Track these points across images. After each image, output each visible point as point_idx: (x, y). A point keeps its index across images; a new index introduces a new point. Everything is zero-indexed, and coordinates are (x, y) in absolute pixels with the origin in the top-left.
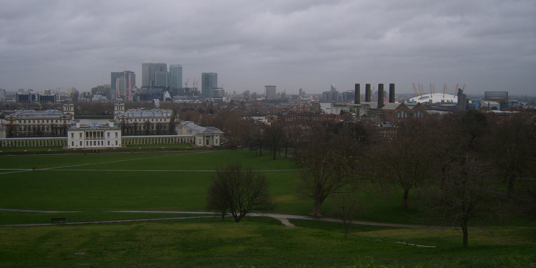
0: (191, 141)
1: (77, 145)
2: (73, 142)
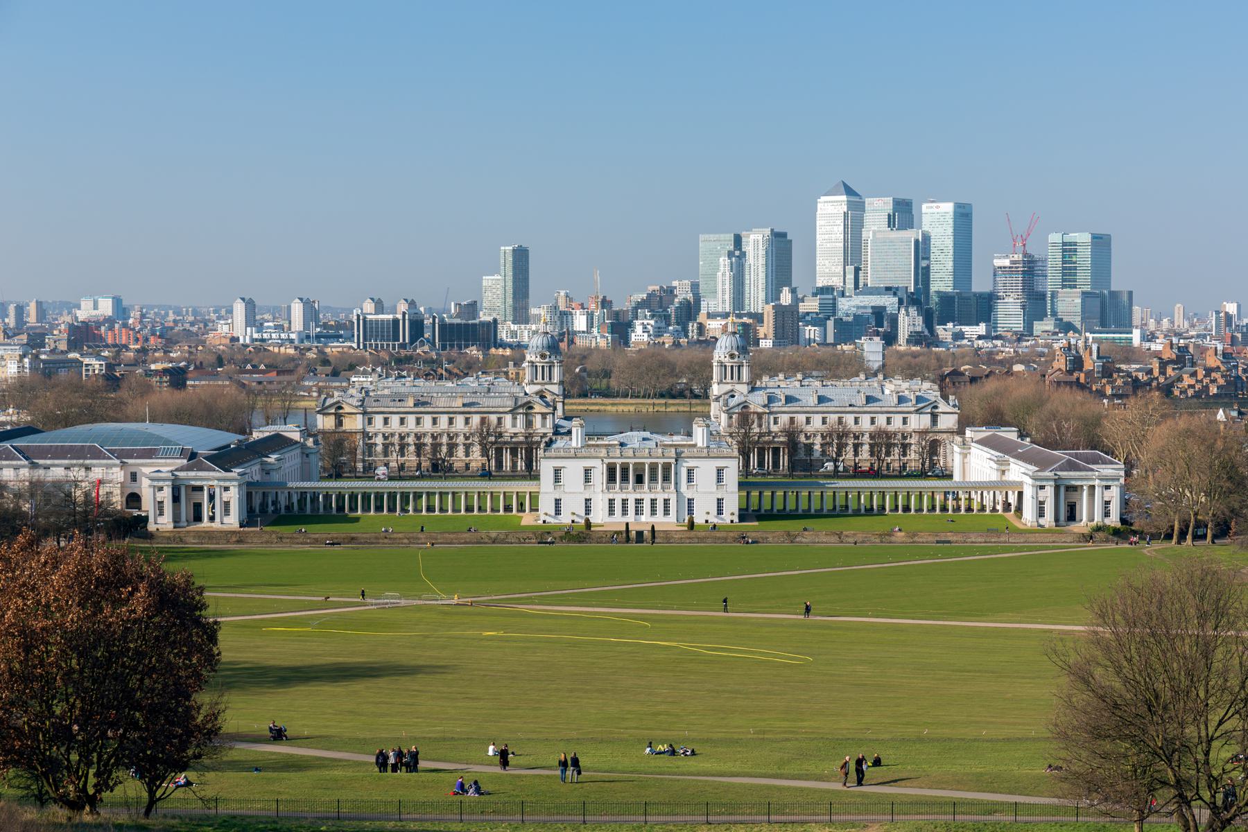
0: (1007, 506)
2: (558, 502)
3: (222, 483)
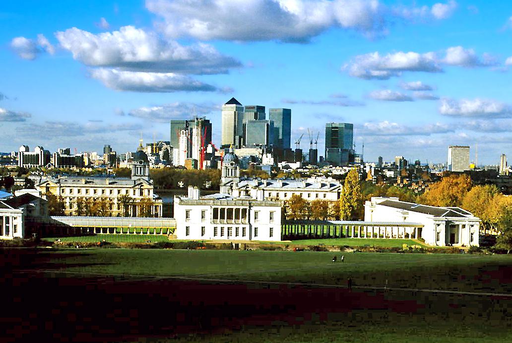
1: (195, 236)
2: (187, 228)
3: (13, 215)
